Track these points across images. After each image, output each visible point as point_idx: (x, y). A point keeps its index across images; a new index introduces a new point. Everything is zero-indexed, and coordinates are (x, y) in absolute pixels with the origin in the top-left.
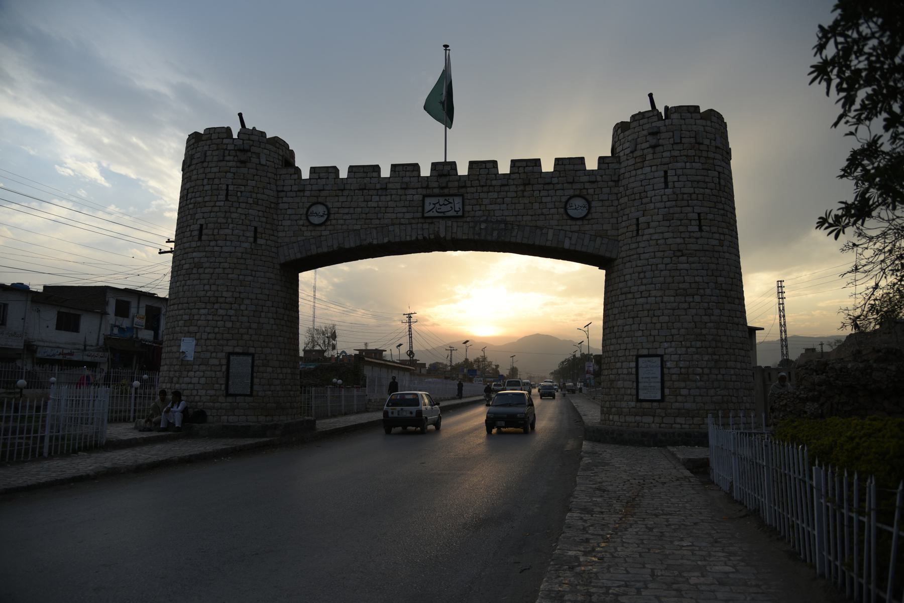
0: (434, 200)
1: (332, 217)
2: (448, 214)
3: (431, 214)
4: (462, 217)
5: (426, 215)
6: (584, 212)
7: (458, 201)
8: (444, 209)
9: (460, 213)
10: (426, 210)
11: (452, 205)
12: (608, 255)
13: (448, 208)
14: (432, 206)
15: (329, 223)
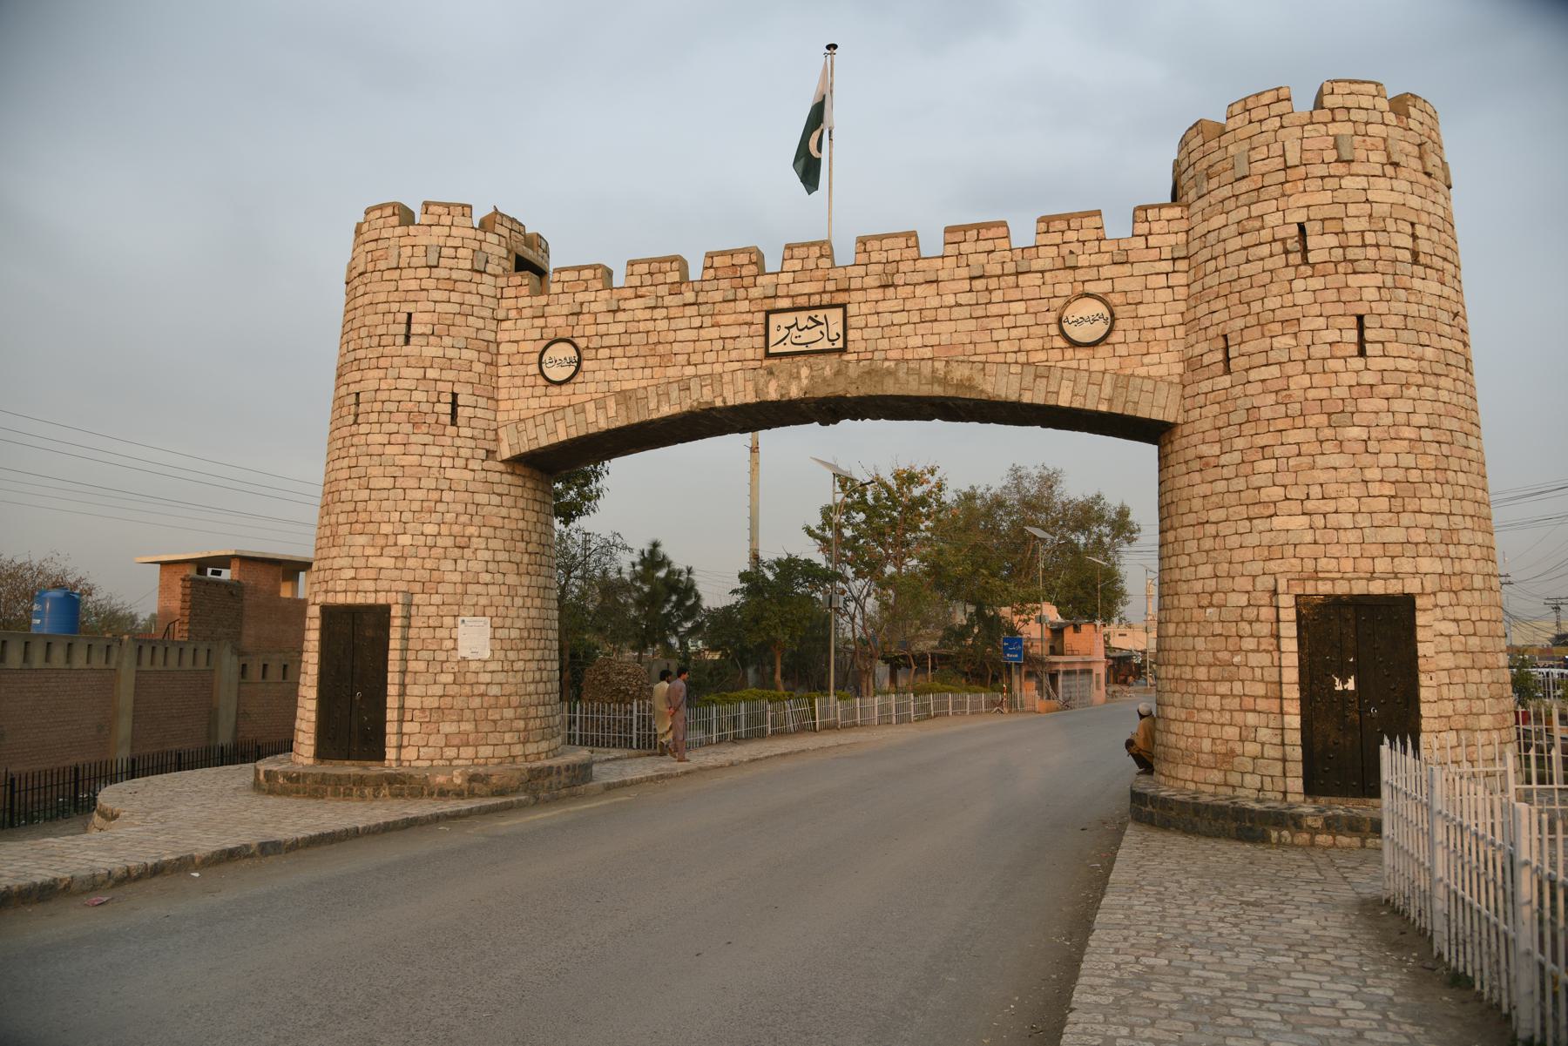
0: (789, 319)
1: (585, 364)
2: (812, 347)
3: (780, 349)
4: (843, 350)
5: (772, 350)
6: (1100, 328)
7: (835, 316)
8: (806, 336)
9: (839, 344)
10: (772, 342)
11: (823, 328)
12: (1157, 415)
13: (815, 334)
14: (784, 332)
15: (579, 378)
